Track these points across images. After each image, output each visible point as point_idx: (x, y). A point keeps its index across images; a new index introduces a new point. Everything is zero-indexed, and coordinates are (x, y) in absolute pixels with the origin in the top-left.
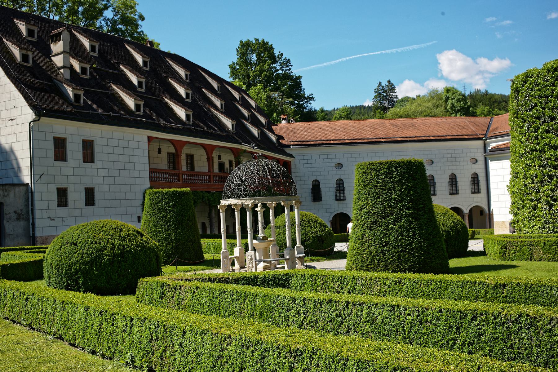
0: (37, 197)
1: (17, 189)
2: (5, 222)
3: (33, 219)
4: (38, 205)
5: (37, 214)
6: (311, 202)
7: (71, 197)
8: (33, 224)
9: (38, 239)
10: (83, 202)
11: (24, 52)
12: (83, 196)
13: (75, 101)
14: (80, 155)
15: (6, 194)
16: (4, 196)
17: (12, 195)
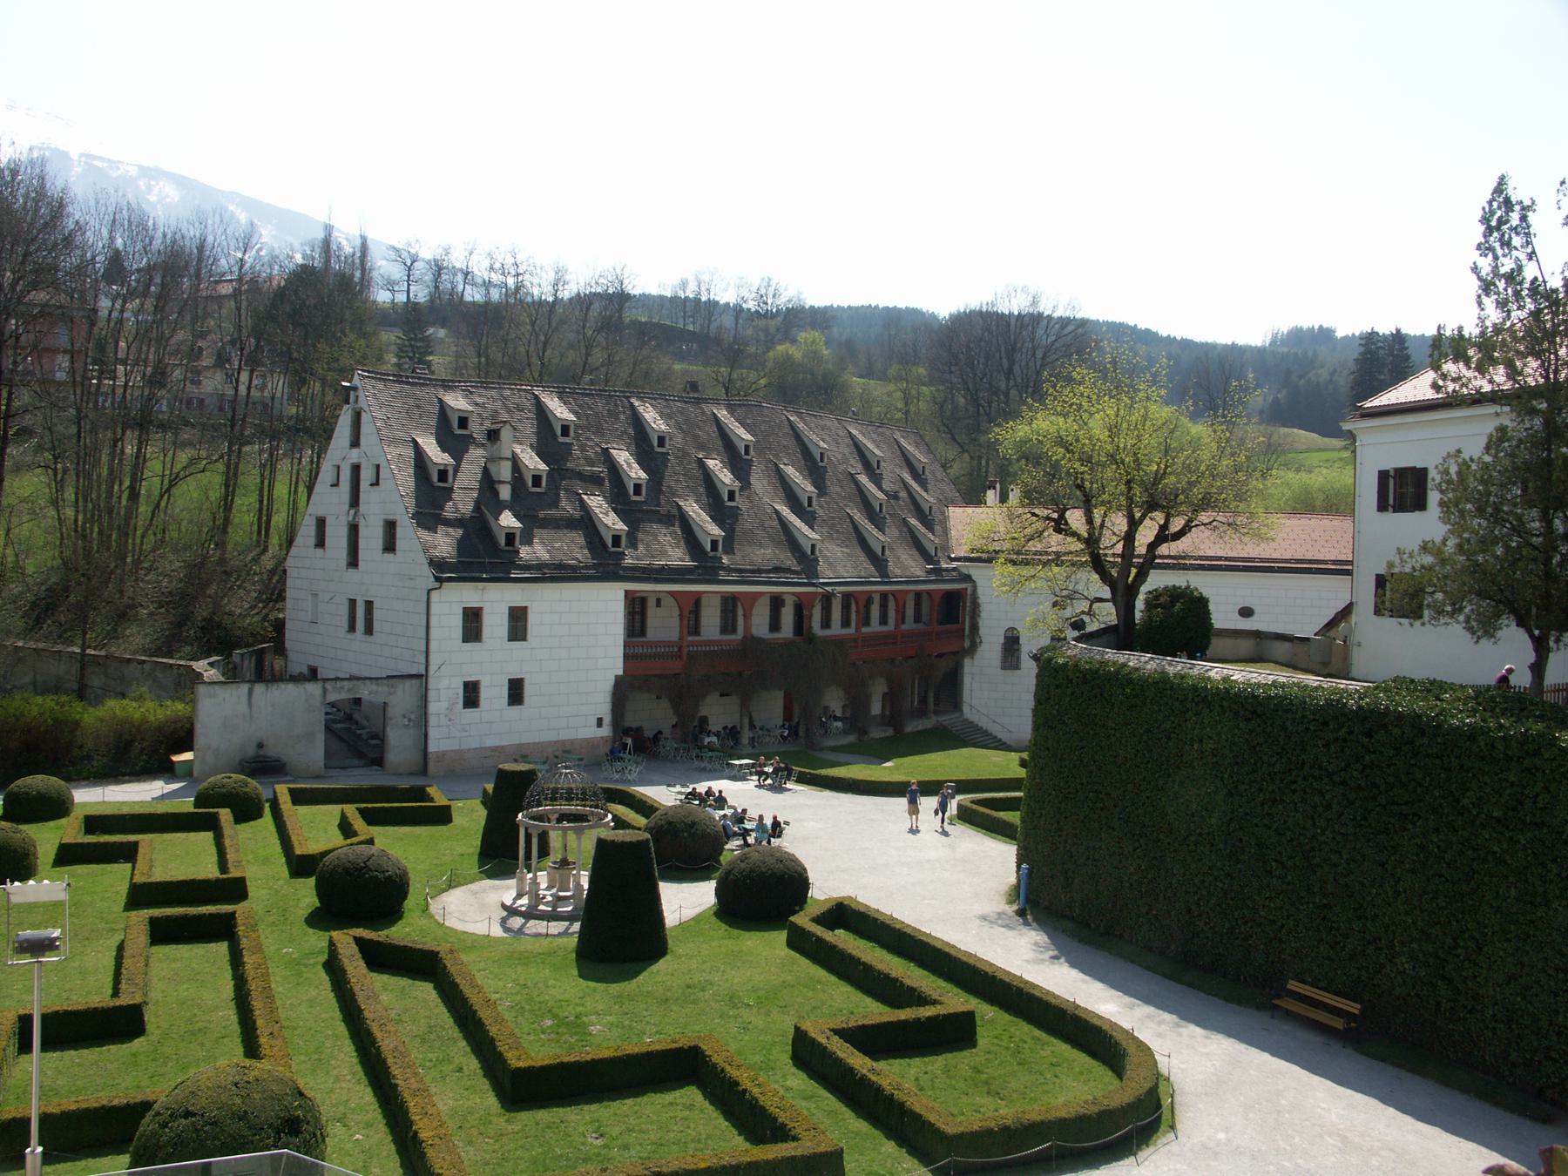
0: (432, 695)
1: (408, 683)
2: (388, 729)
3: (426, 726)
4: (433, 707)
5: (432, 721)
6: (999, 669)
7: (484, 694)
8: (426, 735)
9: (430, 756)
10: (506, 700)
11: (442, 468)
12: (505, 691)
13: (507, 545)
14: (504, 631)
15: (392, 690)
16: (390, 694)
17: (399, 692)
